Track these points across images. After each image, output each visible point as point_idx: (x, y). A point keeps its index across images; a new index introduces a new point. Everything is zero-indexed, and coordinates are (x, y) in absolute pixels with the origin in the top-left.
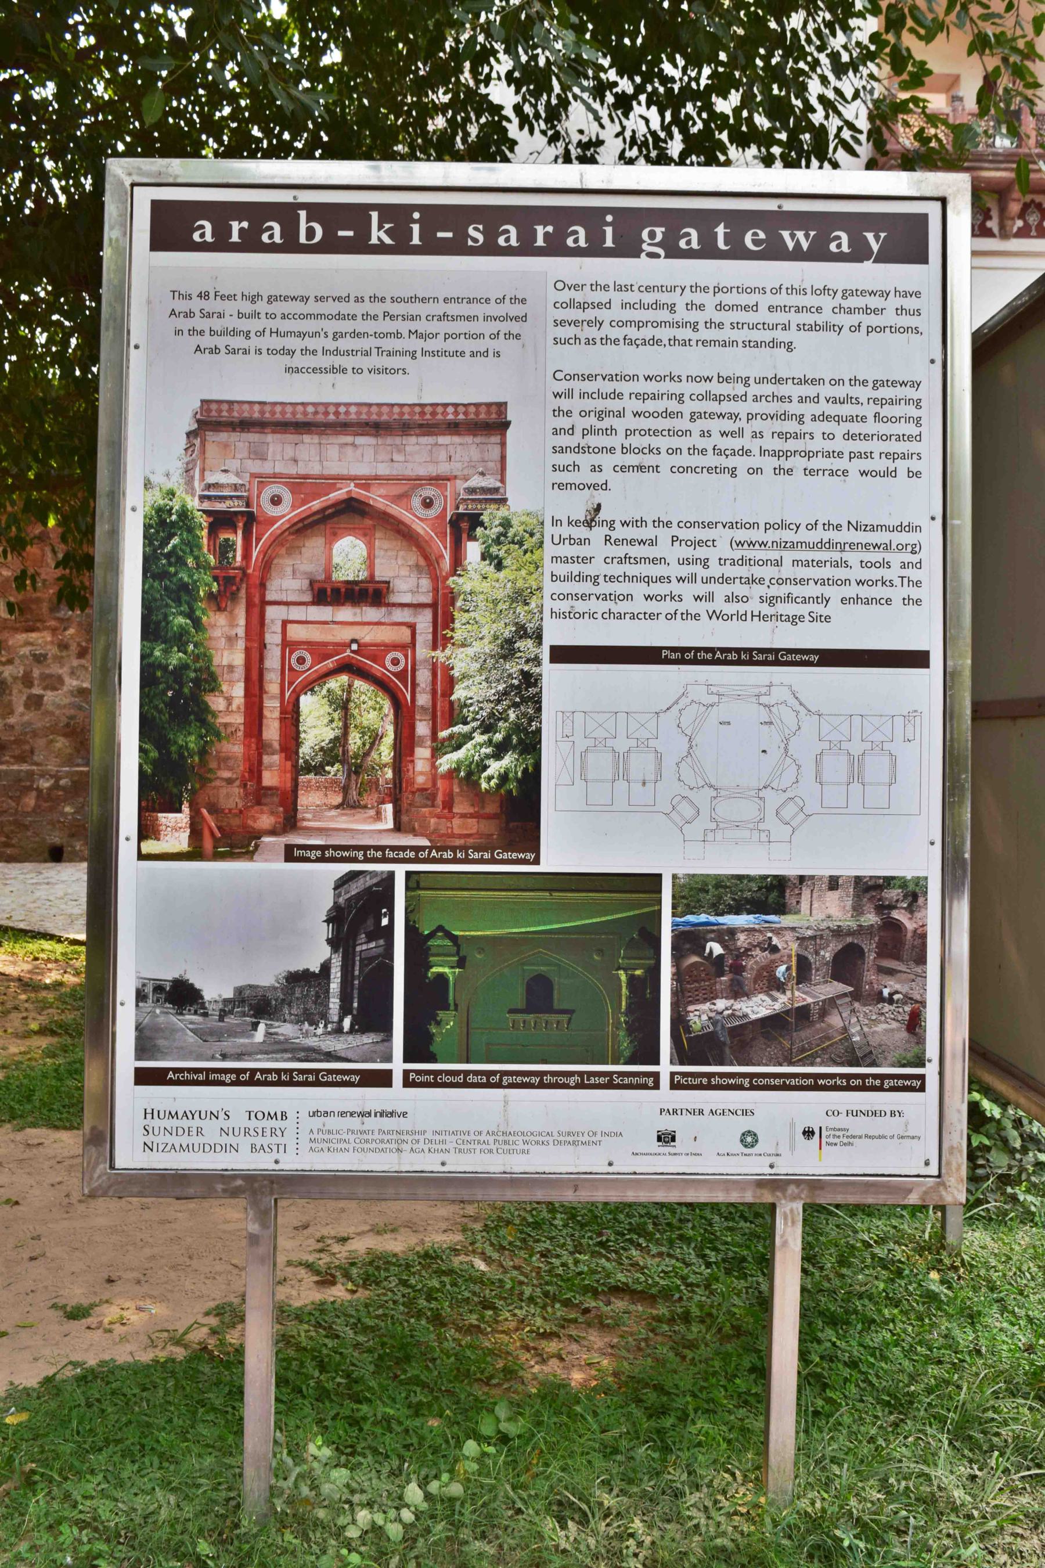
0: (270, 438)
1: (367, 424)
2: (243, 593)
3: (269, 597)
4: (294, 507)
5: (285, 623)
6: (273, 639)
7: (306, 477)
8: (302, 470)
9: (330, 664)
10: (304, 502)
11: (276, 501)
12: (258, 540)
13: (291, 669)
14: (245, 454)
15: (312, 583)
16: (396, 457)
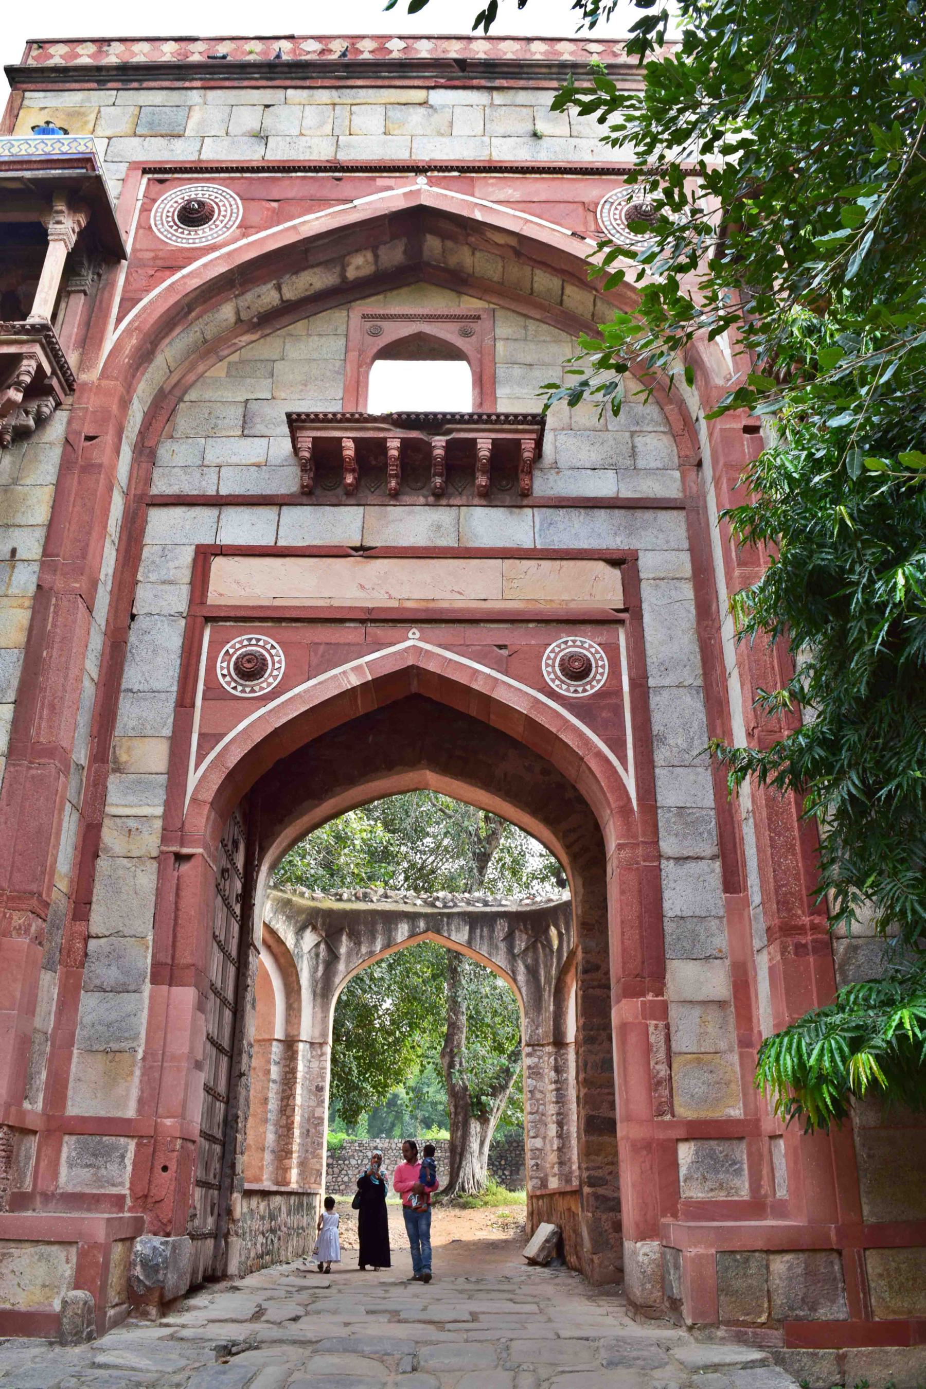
0: (195, 97)
1: (462, 64)
2: (56, 429)
3: (161, 486)
4: (246, 228)
5: (205, 555)
6: (163, 598)
7: (286, 168)
8: (278, 152)
9: (349, 675)
10: (277, 218)
11: (194, 216)
12: (128, 302)
13: (214, 692)
14: (125, 126)
15: (295, 422)
16: (541, 127)
